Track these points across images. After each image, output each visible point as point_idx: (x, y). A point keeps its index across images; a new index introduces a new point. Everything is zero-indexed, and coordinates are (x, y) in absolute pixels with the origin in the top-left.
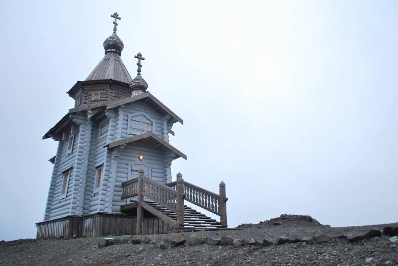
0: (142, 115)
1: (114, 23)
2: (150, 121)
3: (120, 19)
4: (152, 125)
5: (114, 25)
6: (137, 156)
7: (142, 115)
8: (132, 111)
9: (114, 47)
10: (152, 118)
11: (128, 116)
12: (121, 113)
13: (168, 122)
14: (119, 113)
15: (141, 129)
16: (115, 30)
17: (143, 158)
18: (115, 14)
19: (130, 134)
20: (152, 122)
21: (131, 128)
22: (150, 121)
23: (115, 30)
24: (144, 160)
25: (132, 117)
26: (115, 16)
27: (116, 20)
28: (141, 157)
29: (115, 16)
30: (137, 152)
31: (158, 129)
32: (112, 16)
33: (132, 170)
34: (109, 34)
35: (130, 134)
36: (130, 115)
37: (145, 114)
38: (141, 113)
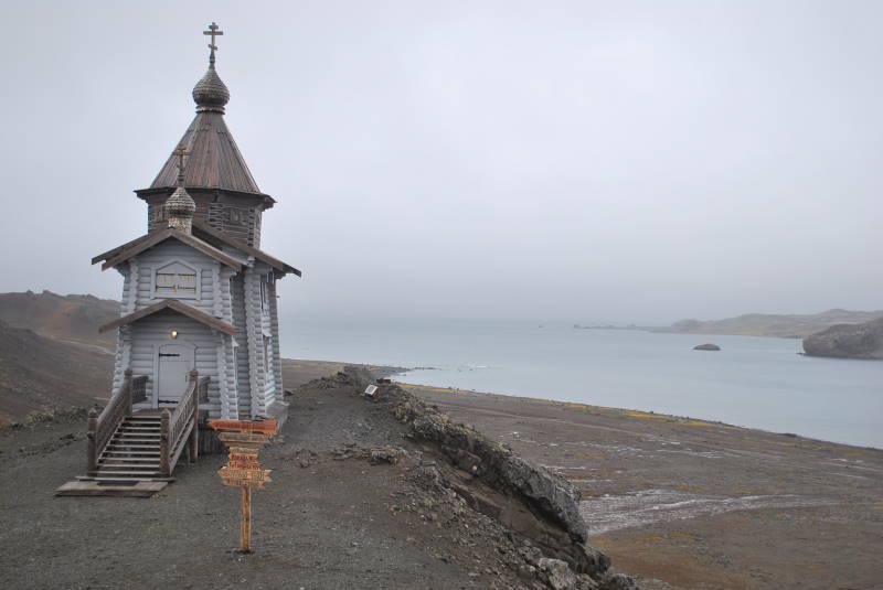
3: (221, 33)
4: (195, 275)
6: (169, 331)
8: (160, 259)
9: (211, 99)
10: (191, 262)
12: (134, 269)
13: (221, 269)
16: (212, 62)
18: (211, 27)
21: (157, 287)
23: (212, 62)
24: (182, 337)
26: (214, 31)
27: (213, 39)
28: (175, 334)
29: (214, 31)
31: (205, 280)
32: (205, 33)
33: (160, 355)
34: (201, 72)
36: (154, 267)
37: (181, 261)
38: (173, 260)
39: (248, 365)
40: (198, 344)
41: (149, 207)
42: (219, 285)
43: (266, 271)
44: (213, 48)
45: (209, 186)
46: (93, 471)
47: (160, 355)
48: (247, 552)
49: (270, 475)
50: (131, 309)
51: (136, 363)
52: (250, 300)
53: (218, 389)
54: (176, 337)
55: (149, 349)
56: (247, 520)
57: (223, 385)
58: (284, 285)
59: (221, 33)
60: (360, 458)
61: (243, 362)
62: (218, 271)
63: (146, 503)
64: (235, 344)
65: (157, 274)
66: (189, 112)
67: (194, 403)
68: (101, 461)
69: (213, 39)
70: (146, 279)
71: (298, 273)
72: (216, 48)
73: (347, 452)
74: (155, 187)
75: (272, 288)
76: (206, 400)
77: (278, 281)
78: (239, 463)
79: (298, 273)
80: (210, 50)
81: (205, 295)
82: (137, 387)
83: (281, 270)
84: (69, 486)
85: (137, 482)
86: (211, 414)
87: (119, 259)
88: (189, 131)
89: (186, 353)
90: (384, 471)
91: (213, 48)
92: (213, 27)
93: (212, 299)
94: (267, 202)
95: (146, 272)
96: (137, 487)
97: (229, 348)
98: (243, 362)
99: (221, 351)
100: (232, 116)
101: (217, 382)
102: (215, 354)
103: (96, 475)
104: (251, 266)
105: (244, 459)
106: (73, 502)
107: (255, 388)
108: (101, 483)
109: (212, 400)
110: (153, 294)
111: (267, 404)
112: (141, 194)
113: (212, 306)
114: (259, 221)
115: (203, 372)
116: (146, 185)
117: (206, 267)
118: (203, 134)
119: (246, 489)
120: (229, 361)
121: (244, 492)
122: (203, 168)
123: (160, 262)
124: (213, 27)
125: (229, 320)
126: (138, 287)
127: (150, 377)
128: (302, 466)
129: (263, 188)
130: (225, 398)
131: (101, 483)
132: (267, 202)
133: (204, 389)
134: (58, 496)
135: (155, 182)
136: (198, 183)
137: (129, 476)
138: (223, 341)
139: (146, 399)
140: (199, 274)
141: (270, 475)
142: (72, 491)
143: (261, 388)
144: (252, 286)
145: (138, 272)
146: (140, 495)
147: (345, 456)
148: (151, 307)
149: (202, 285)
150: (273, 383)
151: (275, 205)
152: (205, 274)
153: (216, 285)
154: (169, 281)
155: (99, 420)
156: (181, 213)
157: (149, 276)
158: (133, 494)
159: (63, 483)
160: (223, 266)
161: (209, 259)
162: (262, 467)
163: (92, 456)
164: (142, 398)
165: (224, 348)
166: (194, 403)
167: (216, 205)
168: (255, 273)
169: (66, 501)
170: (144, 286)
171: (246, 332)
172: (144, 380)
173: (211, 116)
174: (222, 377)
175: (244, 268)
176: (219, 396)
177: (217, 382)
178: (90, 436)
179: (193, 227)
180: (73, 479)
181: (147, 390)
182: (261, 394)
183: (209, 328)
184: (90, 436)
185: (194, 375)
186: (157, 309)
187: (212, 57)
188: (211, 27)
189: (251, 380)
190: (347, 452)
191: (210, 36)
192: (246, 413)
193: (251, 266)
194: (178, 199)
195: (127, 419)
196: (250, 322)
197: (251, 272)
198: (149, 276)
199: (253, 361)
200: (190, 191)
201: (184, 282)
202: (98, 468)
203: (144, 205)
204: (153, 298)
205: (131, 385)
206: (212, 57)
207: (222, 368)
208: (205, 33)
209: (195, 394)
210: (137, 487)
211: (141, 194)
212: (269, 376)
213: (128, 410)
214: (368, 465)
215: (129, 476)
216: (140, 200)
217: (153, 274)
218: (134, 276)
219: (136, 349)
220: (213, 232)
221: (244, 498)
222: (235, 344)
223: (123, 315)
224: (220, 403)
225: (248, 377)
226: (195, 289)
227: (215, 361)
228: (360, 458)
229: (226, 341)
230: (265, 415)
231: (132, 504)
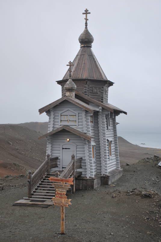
0: (68, 110)
1: (85, 19)
3: (89, 13)
5: (87, 18)
6: (66, 139)
7: (68, 110)
10: (74, 110)
11: (58, 113)
12: (52, 113)
13: (85, 112)
14: (51, 114)
15: (69, 120)
16: (86, 26)
17: (69, 140)
18: (85, 11)
19: (61, 125)
21: (61, 121)
23: (86, 26)
25: (61, 113)
27: (86, 16)
28: (68, 140)
29: (86, 12)
30: (66, 136)
31: (80, 117)
32: (83, 14)
33: (63, 149)
34: (82, 30)
35: (61, 125)
36: (60, 112)
37: (70, 109)
38: (67, 109)
39: (100, 153)
40: (78, 144)
41: (62, 88)
42: (85, 119)
43: (107, 113)
44: (86, 19)
45: (84, 78)
46: (30, 195)
47: (63, 149)
48: (63, 234)
49: (71, 202)
50: (50, 130)
51: (54, 152)
52: (100, 125)
53: (86, 163)
54: (69, 141)
55: (59, 146)
56: (63, 220)
57: (87, 161)
58: (119, 118)
59: (89, 13)
60: (137, 195)
61: (98, 151)
62: (85, 113)
63: (47, 210)
64: (93, 143)
65: (61, 115)
66: (77, 47)
67: (73, 169)
68: (34, 192)
69: (86, 16)
71: (125, 113)
72: (88, 20)
73: (132, 192)
74: (64, 79)
75: (114, 120)
76: (80, 167)
77: (117, 117)
78: (60, 196)
79: (125, 113)
80: (85, 20)
81: (80, 123)
82: (54, 162)
83: (117, 112)
84: (19, 202)
85: (45, 201)
86: (83, 173)
87: (48, 110)
88: (77, 55)
89: (73, 148)
90: (147, 201)
91: (86, 19)
92: (86, 11)
93: (82, 125)
94: (111, 84)
95: (57, 114)
96: (45, 203)
97: (90, 145)
98: (98, 151)
99: (86, 147)
100: (95, 48)
101: (85, 160)
102: (84, 148)
103: (31, 197)
104: (101, 111)
105: (61, 194)
106: (18, 208)
107: (103, 163)
108: (32, 201)
109: (83, 167)
110: (60, 123)
111: (109, 171)
112: (59, 82)
113: (82, 128)
114: (106, 92)
115: (79, 155)
116: (61, 79)
117: (79, 112)
118: (82, 56)
119: (62, 207)
120: (90, 151)
121: (61, 208)
122: (82, 70)
123: (62, 110)
124: (86, 11)
125: (90, 133)
127: (59, 157)
128: (113, 197)
129: (109, 79)
130: (88, 166)
131: (32, 201)
132: (111, 84)
133: (80, 162)
134: (13, 205)
135: (64, 77)
136: (80, 77)
137: (43, 198)
138: (87, 143)
139: (57, 167)
140: (77, 115)
141: (71, 202)
142: (20, 203)
143: (106, 162)
144: (102, 120)
145: (54, 115)
146: (44, 206)
147: (131, 193)
148: (58, 129)
149: (78, 119)
150: (115, 160)
152: (80, 115)
153: (84, 119)
154: (65, 118)
155: (33, 176)
156: (70, 90)
157: (58, 116)
158: (42, 206)
159: (19, 200)
160: (87, 111)
161: (80, 108)
162: (68, 198)
163: (30, 190)
164: (56, 166)
165: (88, 146)
166: (73, 169)
167: (86, 86)
168: (103, 114)
169: (15, 207)
170: (56, 120)
171: (99, 139)
172: (57, 158)
173: (86, 48)
174: (87, 158)
175: (98, 112)
177: (85, 160)
178: (28, 181)
179: (75, 95)
180: (22, 199)
181: (58, 163)
182: (106, 165)
183: (80, 137)
184: (28, 181)
185: (73, 157)
186: (60, 130)
187: (86, 24)
188: (85, 11)
189: (101, 159)
190: (132, 192)
191: (85, 15)
192: (98, 174)
193: (101, 111)
194: (68, 85)
195: (47, 175)
196: (101, 134)
197: (101, 113)
198: (58, 116)
199: (102, 151)
200: (73, 80)
201: (72, 118)
202: (33, 194)
203: (60, 87)
204: (59, 125)
205: (49, 160)
206: (86, 24)
207: (87, 154)
208: (83, 14)
209: (74, 163)
210: (45, 203)
211: (59, 82)
212: (113, 157)
213: (48, 171)
214: (140, 198)
215: (43, 198)
216: (58, 85)
217: (60, 115)
218: (52, 116)
219: (54, 146)
220: (86, 97)
221: (61, 211)
222: (93, 143)
223: (48, 132)
225: (100, 158)
227: (84, 151)
228: (137, 195)
229: (88, 143)
230: (107, 174)
231: (39, 210)
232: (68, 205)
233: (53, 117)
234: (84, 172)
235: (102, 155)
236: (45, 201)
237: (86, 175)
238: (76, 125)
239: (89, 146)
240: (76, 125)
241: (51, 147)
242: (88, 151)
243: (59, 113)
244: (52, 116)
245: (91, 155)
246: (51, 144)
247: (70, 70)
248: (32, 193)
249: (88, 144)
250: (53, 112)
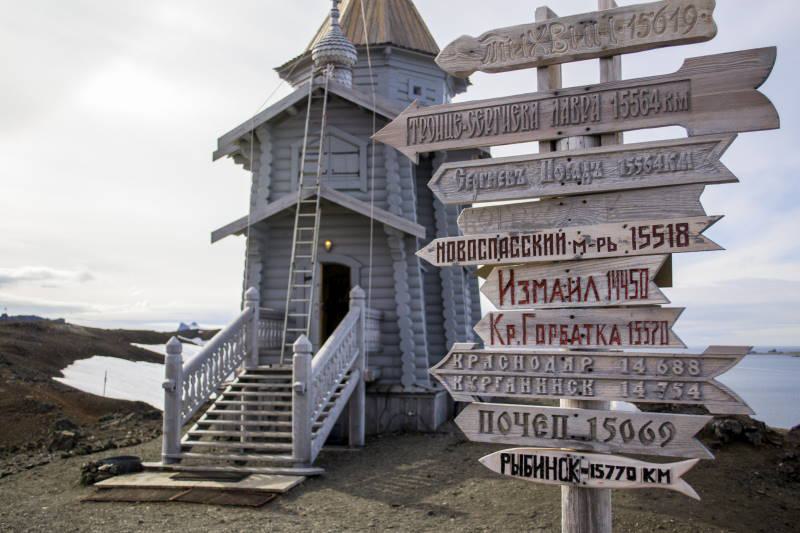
2: (356, 146)
4: (358, 153)
10: (354, 134)
11: (290, 148)
12: (267, 147)
14: (262, 147)
20: (358, 147)
22: (356, 146)
28: (328, 243)
53: (397, 331)
70: (283, 164)
95: (283, 153)
102: (391, 275)
126: (271, 176)
138: (404, 255)
140: (363, 153)
145: (272, 152)
151: (469, 88)
170: (283, 175)
176: (397, 343)
195: (248, 372)
198: (290, 159)
219: (270, 273)
224: (401, 354)
226: (358, 173)
229: (408, 254)
232: (702, 421)
233: (270, 161)
234: (390, 367)
235: (450, 312)
236: (246, 475)
237: (399, 378)
238: (358, 190)
239: (409, 265)
240: (358, 190)
241: (262, 272)
242: (407, 286)
243: (292, 145)
244: (266, 170)
245: (416, 301)
246: (263, 262)
247: (335, 14)
248: (184, 440)
249: (406, 259)
250: (275, 140)
